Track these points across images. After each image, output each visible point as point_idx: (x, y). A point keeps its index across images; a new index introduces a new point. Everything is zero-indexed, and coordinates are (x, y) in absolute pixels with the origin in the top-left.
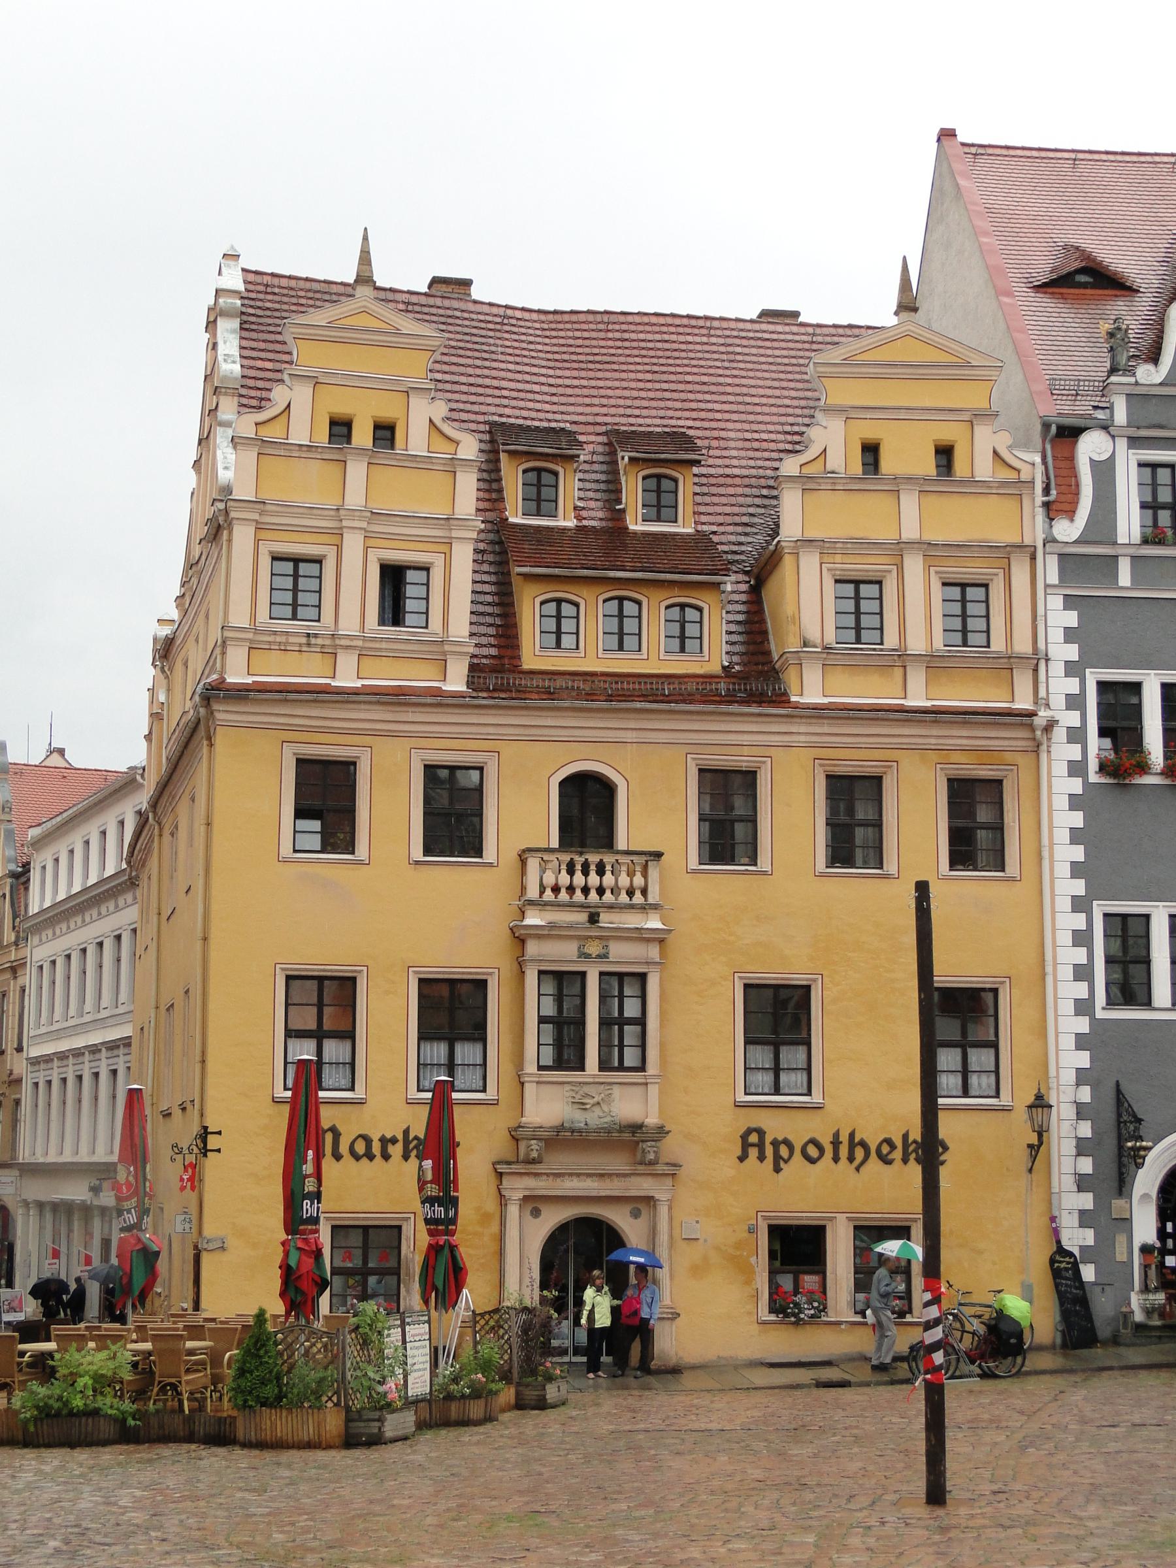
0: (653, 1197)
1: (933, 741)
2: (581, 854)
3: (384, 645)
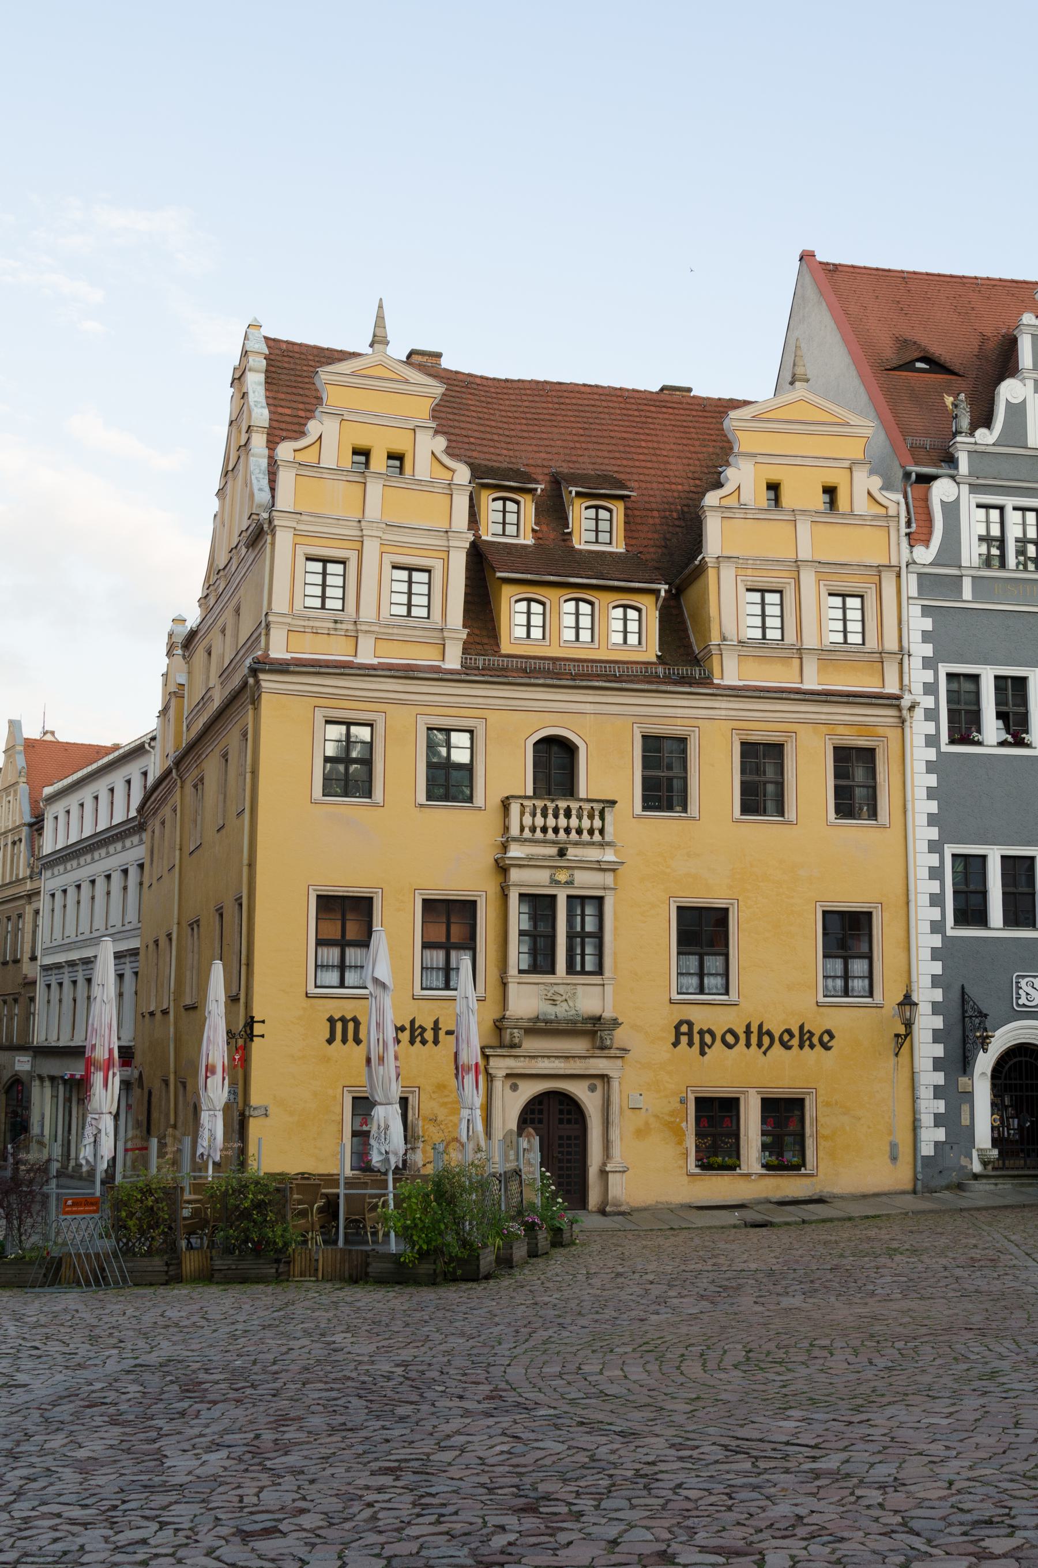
1: (823, 717)
2: (553, 801)
3: (395, 631)
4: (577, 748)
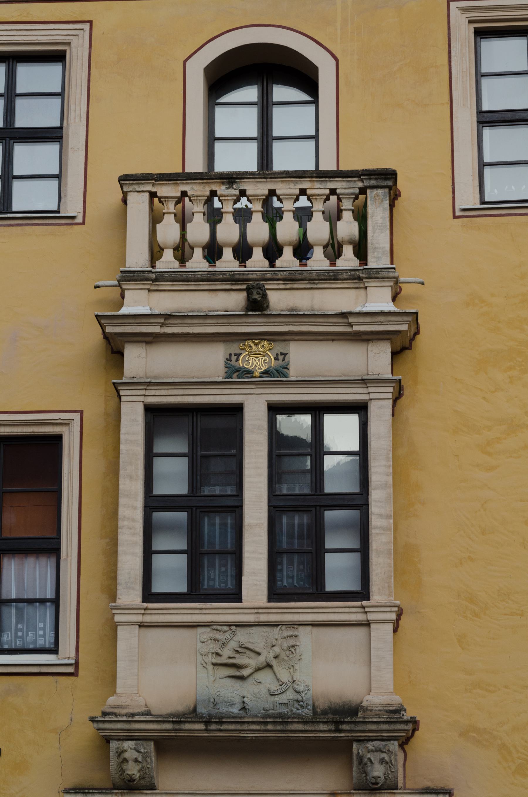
4: (315, 69)
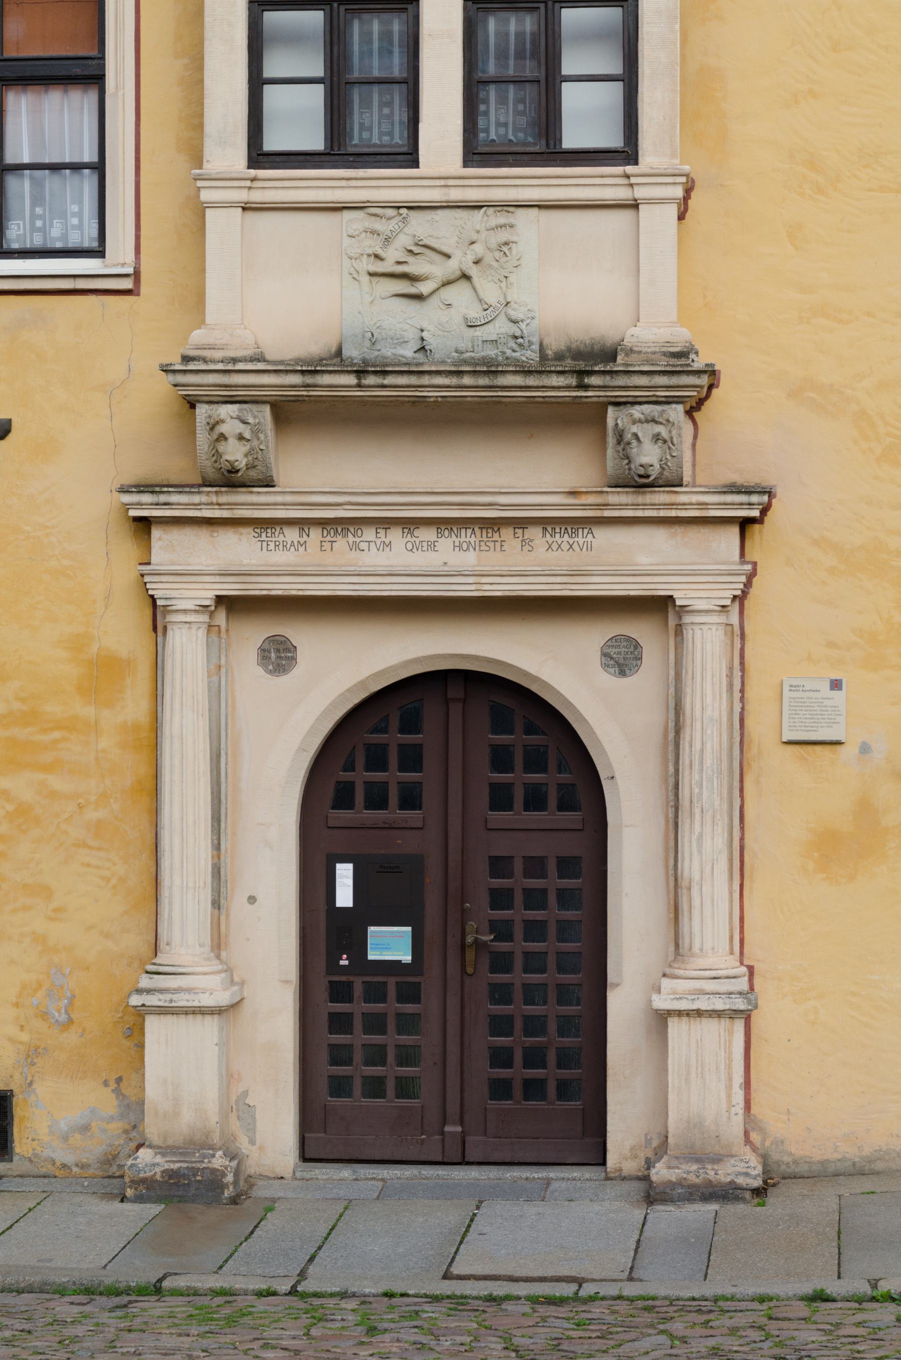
0: (671, 597)
